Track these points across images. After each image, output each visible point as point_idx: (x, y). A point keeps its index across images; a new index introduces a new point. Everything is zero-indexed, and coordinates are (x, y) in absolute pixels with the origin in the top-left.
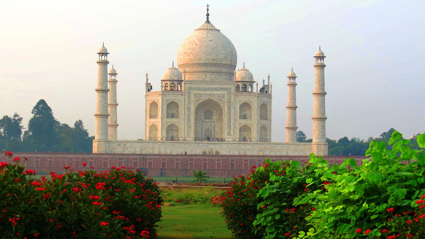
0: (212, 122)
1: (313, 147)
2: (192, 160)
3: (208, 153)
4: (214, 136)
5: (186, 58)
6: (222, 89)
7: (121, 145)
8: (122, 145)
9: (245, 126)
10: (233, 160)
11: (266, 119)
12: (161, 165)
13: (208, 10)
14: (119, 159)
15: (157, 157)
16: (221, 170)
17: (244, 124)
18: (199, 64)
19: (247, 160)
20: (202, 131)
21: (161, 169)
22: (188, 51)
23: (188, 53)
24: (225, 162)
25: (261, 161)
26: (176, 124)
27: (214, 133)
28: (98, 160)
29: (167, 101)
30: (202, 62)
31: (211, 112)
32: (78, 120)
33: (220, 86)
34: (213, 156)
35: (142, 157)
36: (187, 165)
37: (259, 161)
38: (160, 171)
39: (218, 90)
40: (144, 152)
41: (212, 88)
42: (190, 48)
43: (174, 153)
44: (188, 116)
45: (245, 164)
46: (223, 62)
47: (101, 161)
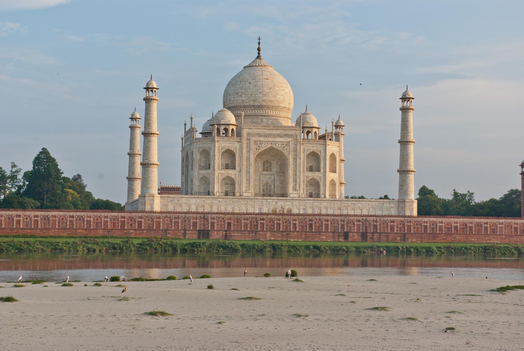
0: (271, 175)
1: (400, 205)
2: (263, 219)
3: (278, 212)
4: (274, 191)
5: (238, 98)
6: (286, 135)
8: (176, 200)
9: (313, 179)
10: (312, 220)
11: (335, 172)
12: (226, 225)
13: (259, 43)
14: (175, 218)
15: (221, 215)
16: (298, 232)
17: (312, 177)
18: (254, 106)
19: (328, 221)
20: (260, 186)
21: (226, 231)
22: (240, 91)
23: (240, 94)
24: (302, 222)
25: (344, 221)
26: (233, 176)
27: (274, 187)
28: (149, 220)
29: (222, 149)
30: (257, 104)
31: (270, 163)
32: (76, 174)
33: (284, 132)
34: (283, 214)
35: (202, 216)
36: (257, 225)
37: (341, 221)
38: (224, 233)
39: (281, 137)
40: (201, 210)
41: (274, 134)
42: (242, 87)
43: (237, 211)
44: (247, 167)
45: (326, 224)
46: (281, 105)
47: (152, 221)
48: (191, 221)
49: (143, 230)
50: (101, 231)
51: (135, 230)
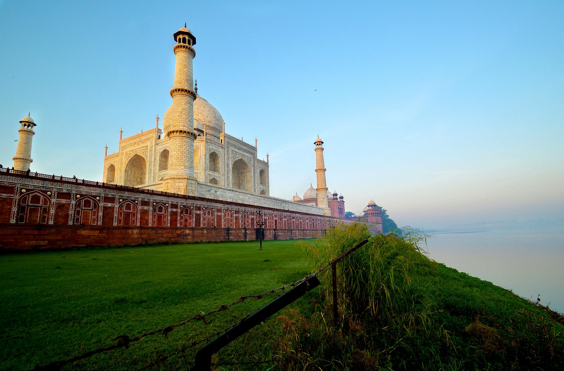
7: (211, 192)
21: (275, 230)
48: (250, 217)
49: (202, 229)
50: (135, 231)
51: (192, 229)
